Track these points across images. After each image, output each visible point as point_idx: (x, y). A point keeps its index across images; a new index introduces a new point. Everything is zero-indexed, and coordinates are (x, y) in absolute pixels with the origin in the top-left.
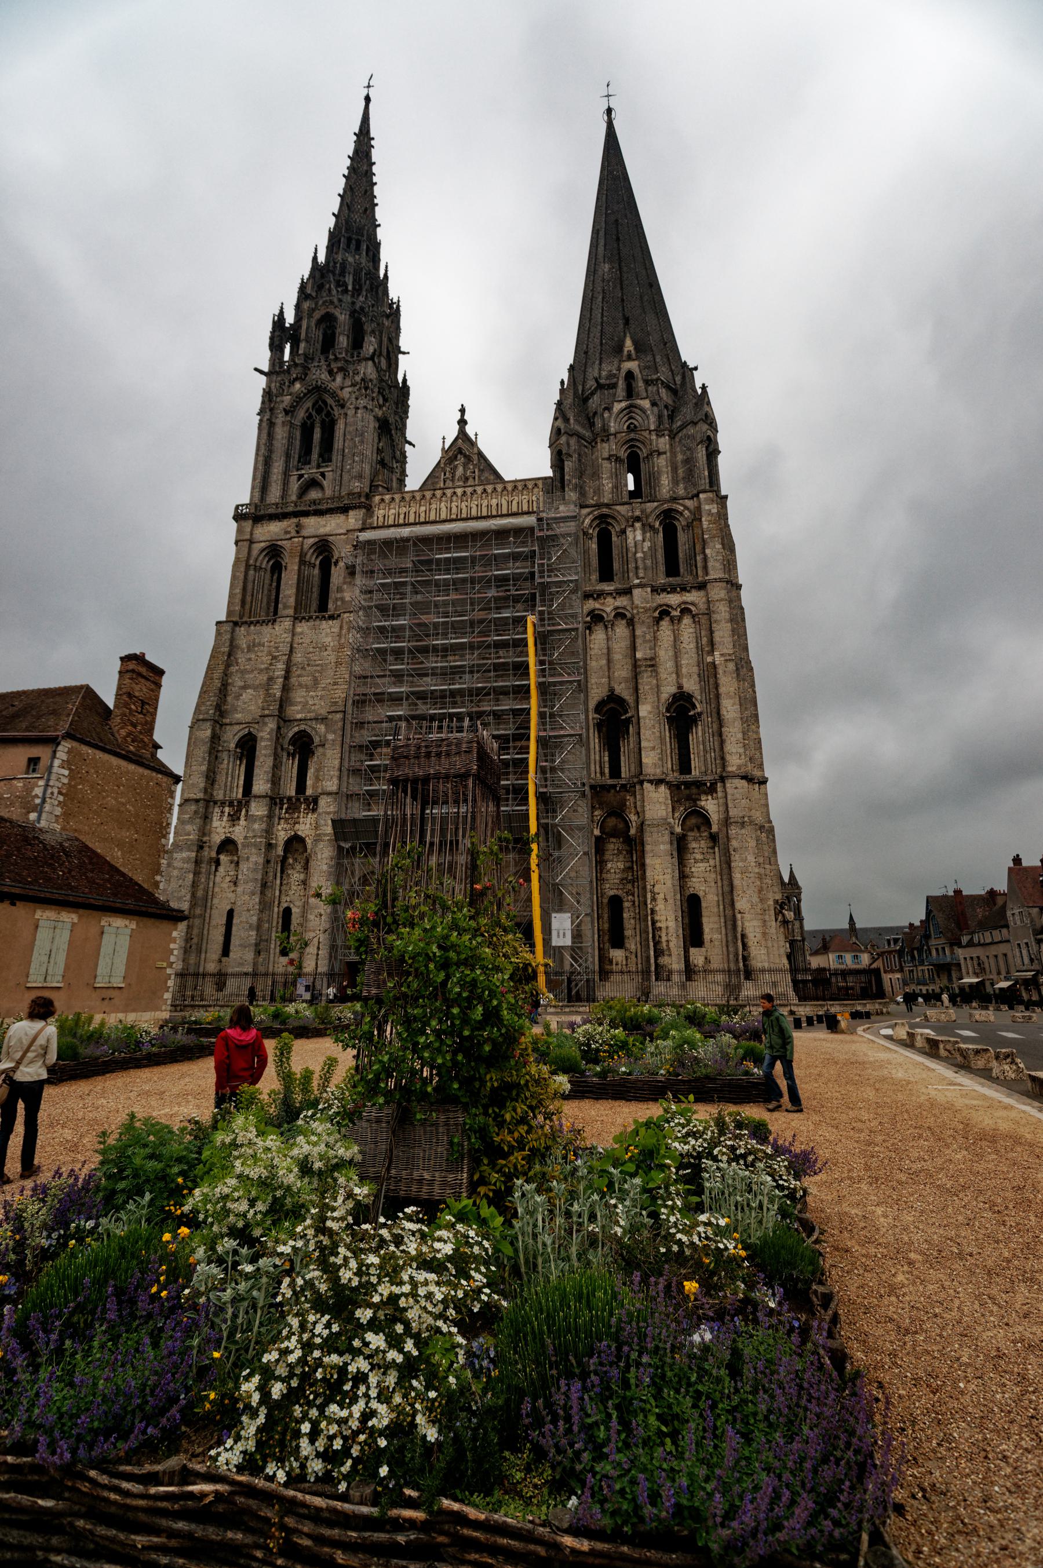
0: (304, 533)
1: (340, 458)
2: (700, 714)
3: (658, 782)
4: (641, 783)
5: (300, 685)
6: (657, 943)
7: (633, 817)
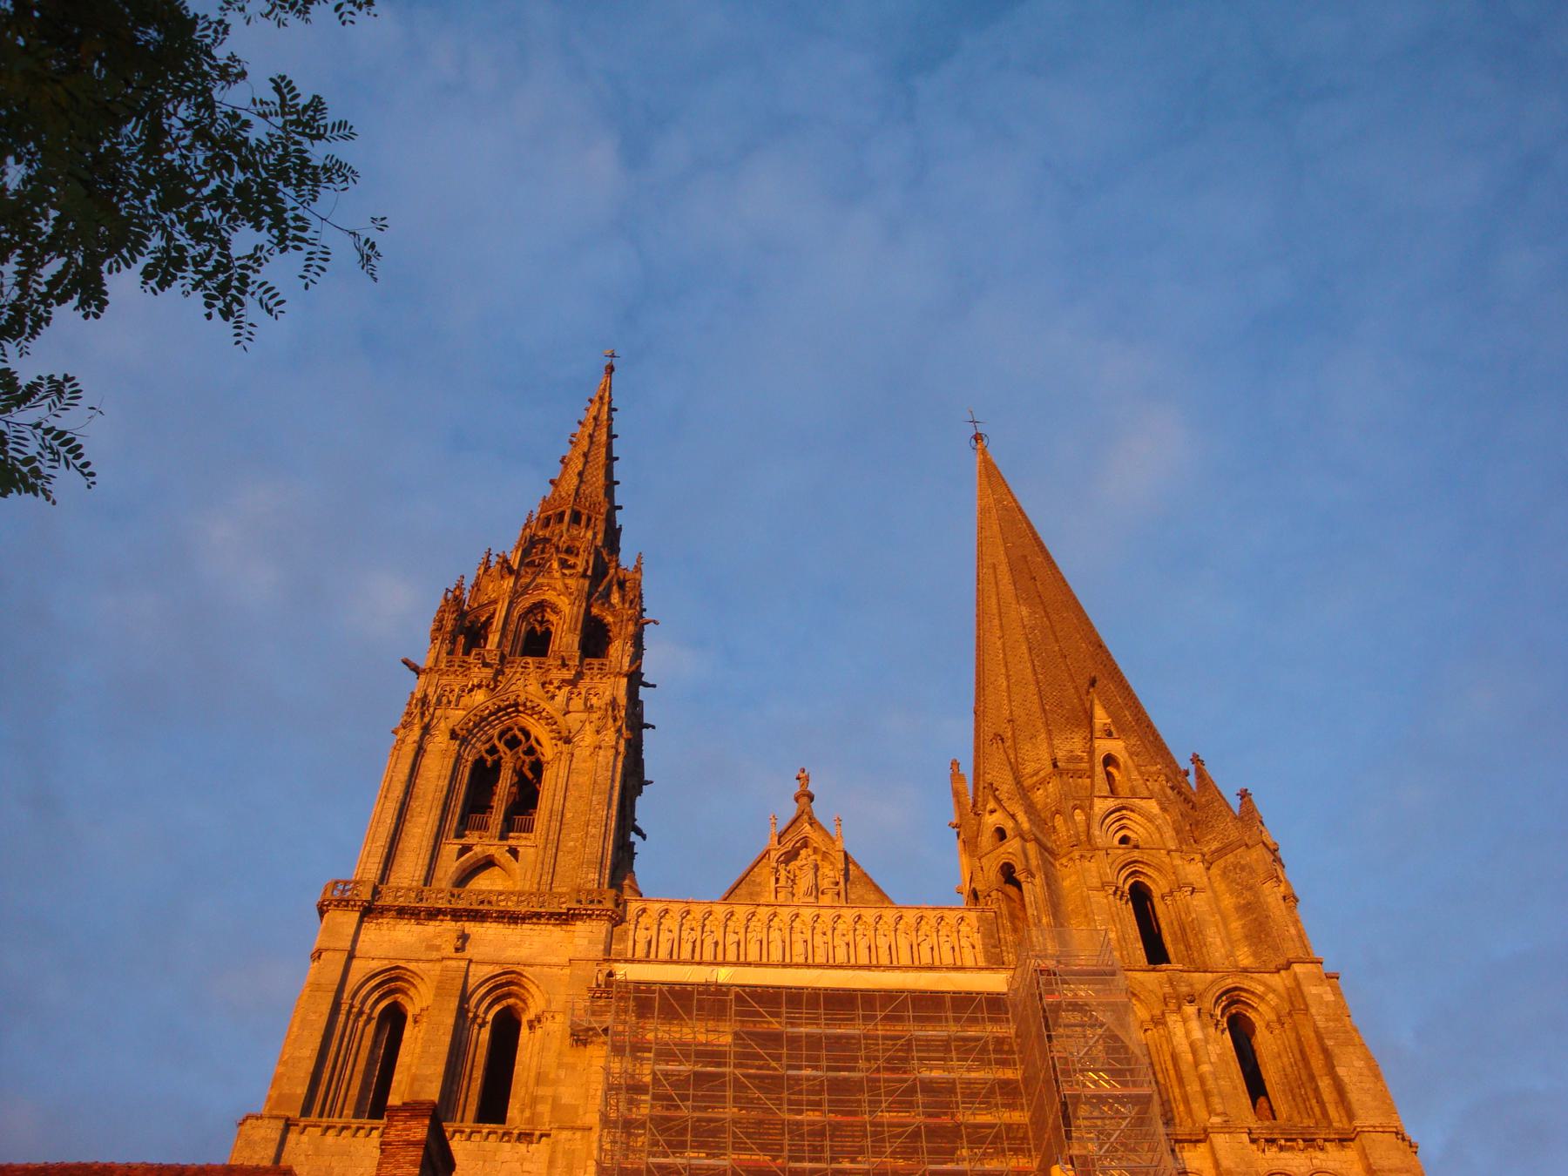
1: (555, 825)
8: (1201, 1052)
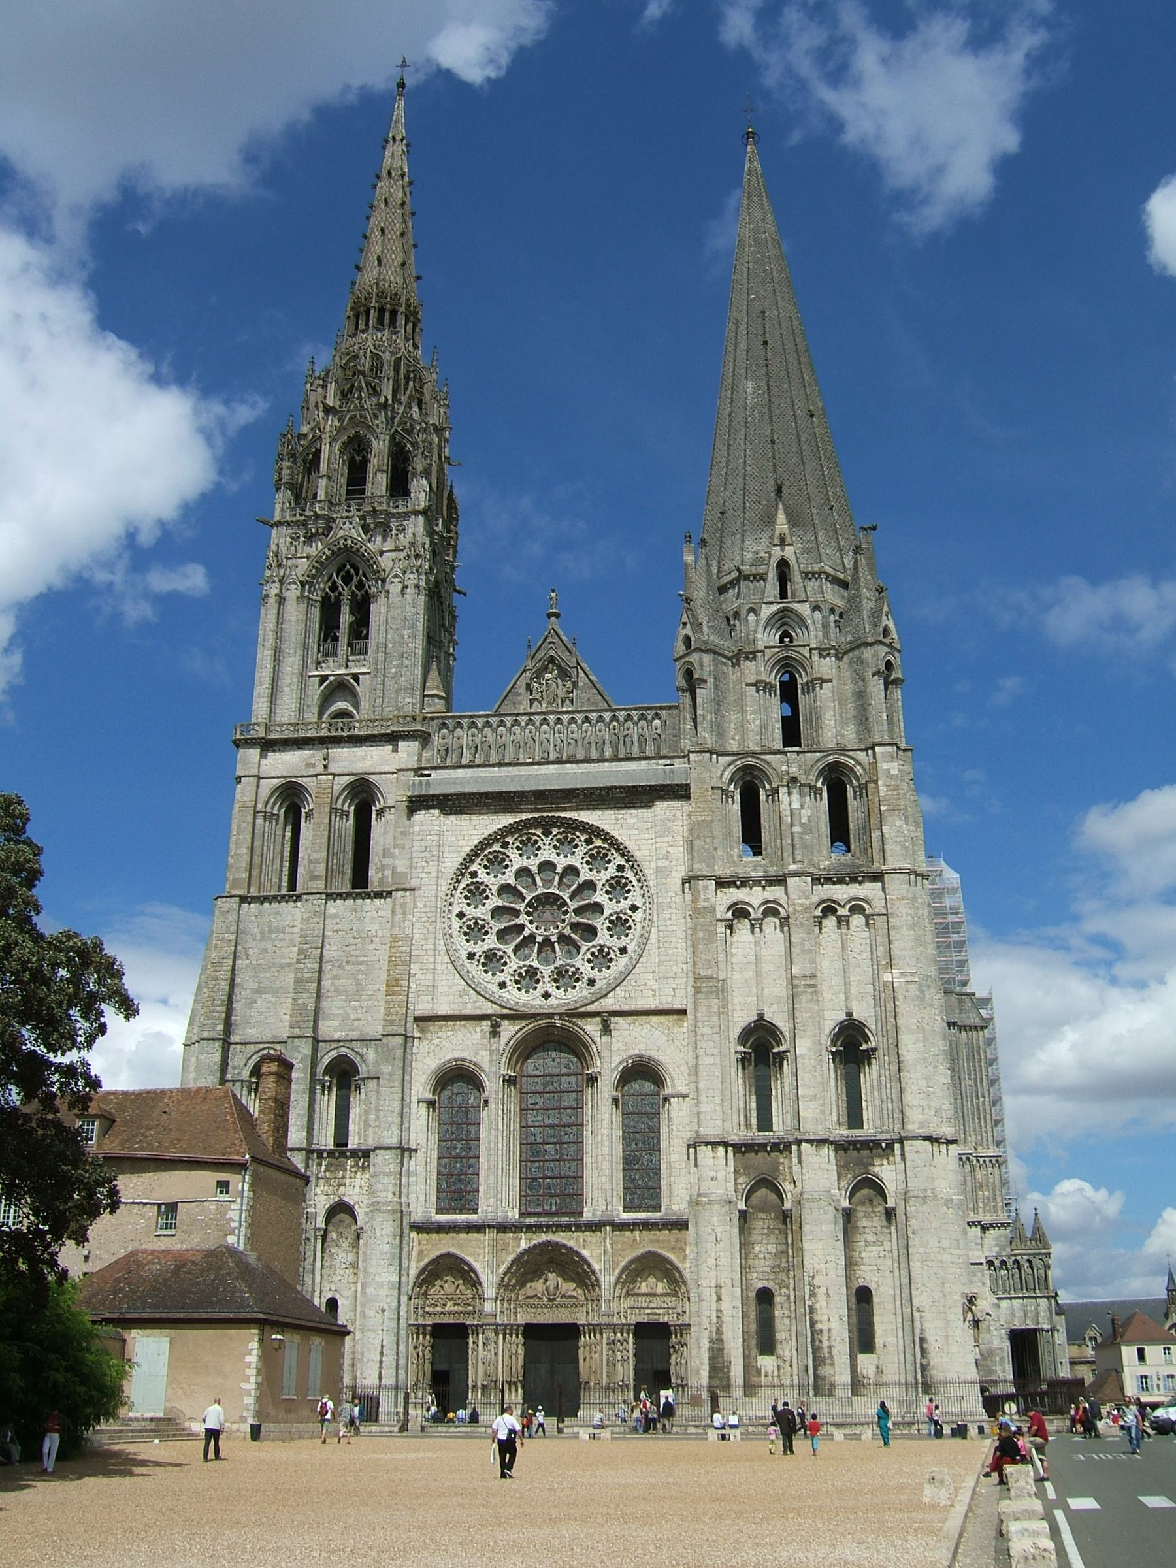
0: (333, 768)
1: (381, 656)
2: (874, 1050)
3: (821, 1142)
4: (799, 1143)
5: (337, 991)
6: (816, 1350)
7: (788, 1187)
8: (796, 818)
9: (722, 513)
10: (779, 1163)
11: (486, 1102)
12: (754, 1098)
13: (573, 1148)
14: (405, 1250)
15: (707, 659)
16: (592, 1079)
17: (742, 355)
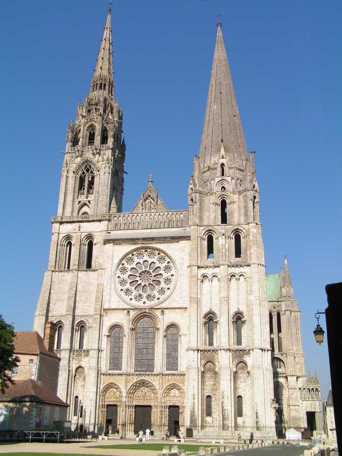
1: (97, 195)
4: (221, 350)
6: (223, 415)
7: (217, 364)
9: (205, 148)
10: (213, 357)
11: (125, 336)
12: (208, 336)
13: (151, 351)
14: (99, 382)
15: (198, 195)
16: (158, 329)
17: (213, 96)
